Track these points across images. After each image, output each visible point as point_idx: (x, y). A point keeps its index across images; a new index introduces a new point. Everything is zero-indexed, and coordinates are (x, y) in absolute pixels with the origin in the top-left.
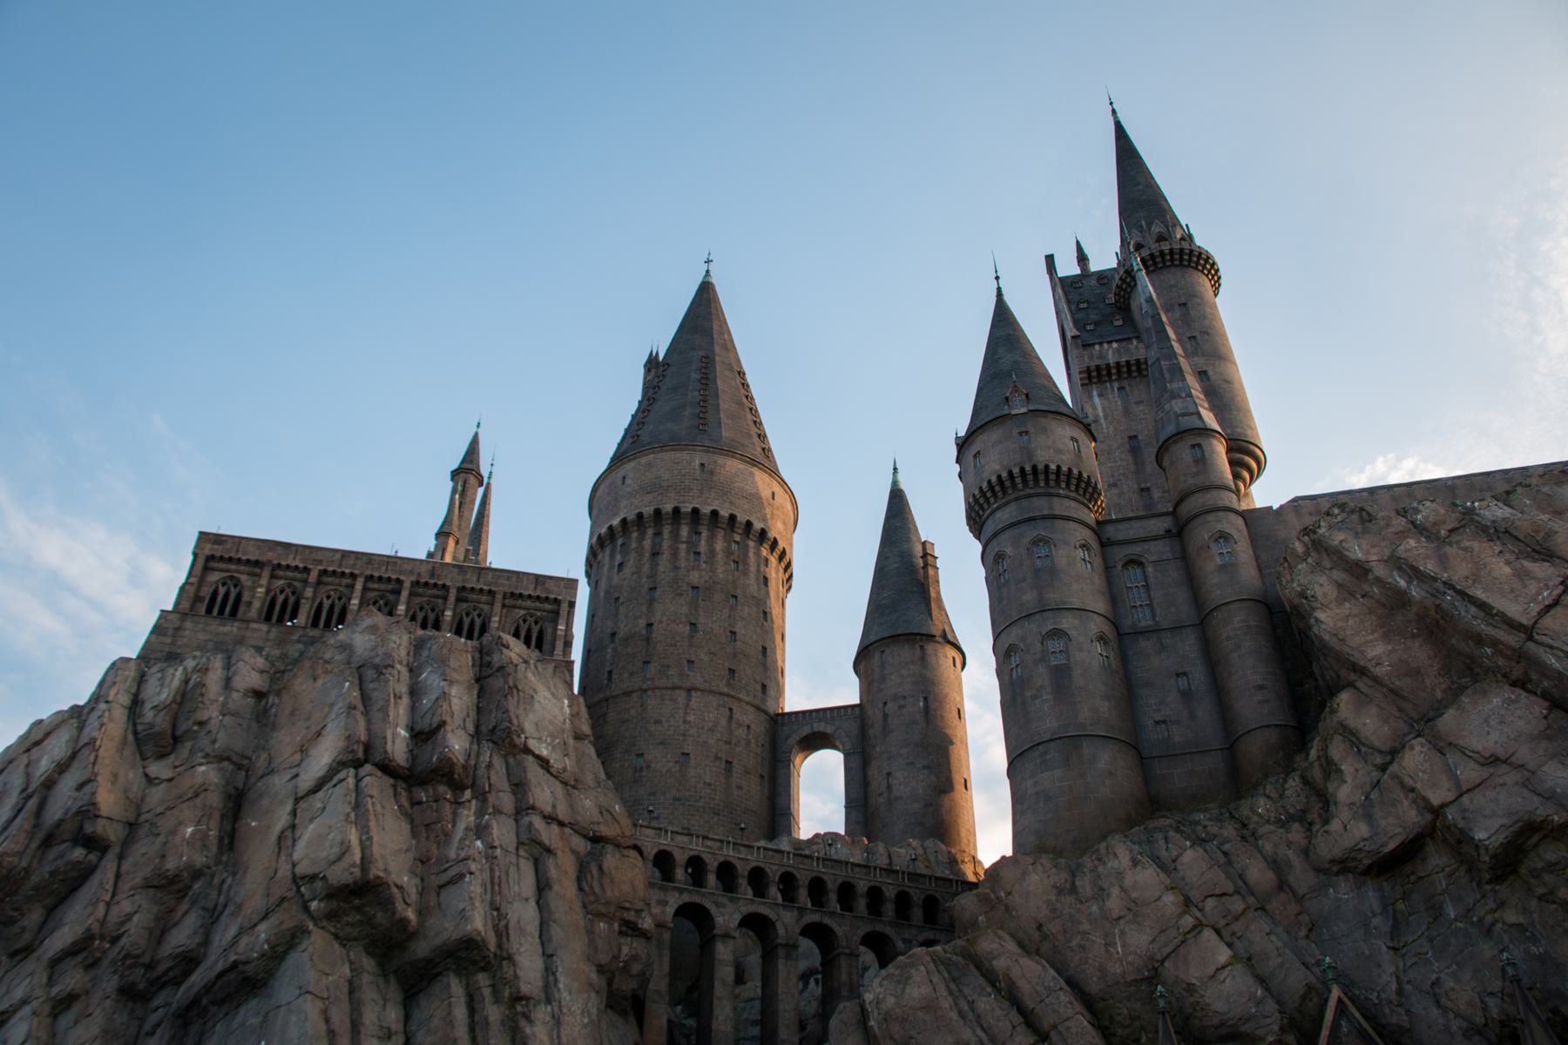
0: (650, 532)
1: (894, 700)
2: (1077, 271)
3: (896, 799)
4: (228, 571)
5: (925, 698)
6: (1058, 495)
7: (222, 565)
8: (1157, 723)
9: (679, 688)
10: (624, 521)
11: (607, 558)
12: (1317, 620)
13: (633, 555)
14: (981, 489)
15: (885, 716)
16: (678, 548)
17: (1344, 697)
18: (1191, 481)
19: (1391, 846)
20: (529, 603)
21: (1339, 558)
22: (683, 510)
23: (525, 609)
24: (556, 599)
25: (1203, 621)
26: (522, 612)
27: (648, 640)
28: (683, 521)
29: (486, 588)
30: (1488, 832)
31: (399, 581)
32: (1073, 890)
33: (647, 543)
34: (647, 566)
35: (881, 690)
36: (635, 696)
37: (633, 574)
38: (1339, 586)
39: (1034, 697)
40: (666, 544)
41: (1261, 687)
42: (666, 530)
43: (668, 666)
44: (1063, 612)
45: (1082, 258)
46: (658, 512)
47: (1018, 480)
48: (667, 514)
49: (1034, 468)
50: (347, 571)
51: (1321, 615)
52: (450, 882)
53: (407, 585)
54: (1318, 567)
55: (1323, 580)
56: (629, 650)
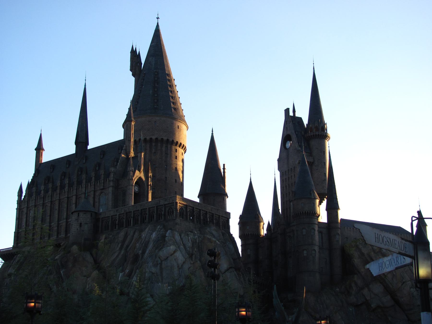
0: (164, 145)
10: (157, 139)
12: (354, 260)
14: (303, 212)
17: (356, 276)
19: (359, 304)
20: (223, 218)
23: (223, 219)
24: (228, 218)
26: (222, 220)
29: (219, 214)
30: (373, 306)
31: (207, 212)
33: (164, 149)
42: (169, 146)
46: (168, 140)
47: (311, 214)
50: (199, 208)
53: (208, 213)
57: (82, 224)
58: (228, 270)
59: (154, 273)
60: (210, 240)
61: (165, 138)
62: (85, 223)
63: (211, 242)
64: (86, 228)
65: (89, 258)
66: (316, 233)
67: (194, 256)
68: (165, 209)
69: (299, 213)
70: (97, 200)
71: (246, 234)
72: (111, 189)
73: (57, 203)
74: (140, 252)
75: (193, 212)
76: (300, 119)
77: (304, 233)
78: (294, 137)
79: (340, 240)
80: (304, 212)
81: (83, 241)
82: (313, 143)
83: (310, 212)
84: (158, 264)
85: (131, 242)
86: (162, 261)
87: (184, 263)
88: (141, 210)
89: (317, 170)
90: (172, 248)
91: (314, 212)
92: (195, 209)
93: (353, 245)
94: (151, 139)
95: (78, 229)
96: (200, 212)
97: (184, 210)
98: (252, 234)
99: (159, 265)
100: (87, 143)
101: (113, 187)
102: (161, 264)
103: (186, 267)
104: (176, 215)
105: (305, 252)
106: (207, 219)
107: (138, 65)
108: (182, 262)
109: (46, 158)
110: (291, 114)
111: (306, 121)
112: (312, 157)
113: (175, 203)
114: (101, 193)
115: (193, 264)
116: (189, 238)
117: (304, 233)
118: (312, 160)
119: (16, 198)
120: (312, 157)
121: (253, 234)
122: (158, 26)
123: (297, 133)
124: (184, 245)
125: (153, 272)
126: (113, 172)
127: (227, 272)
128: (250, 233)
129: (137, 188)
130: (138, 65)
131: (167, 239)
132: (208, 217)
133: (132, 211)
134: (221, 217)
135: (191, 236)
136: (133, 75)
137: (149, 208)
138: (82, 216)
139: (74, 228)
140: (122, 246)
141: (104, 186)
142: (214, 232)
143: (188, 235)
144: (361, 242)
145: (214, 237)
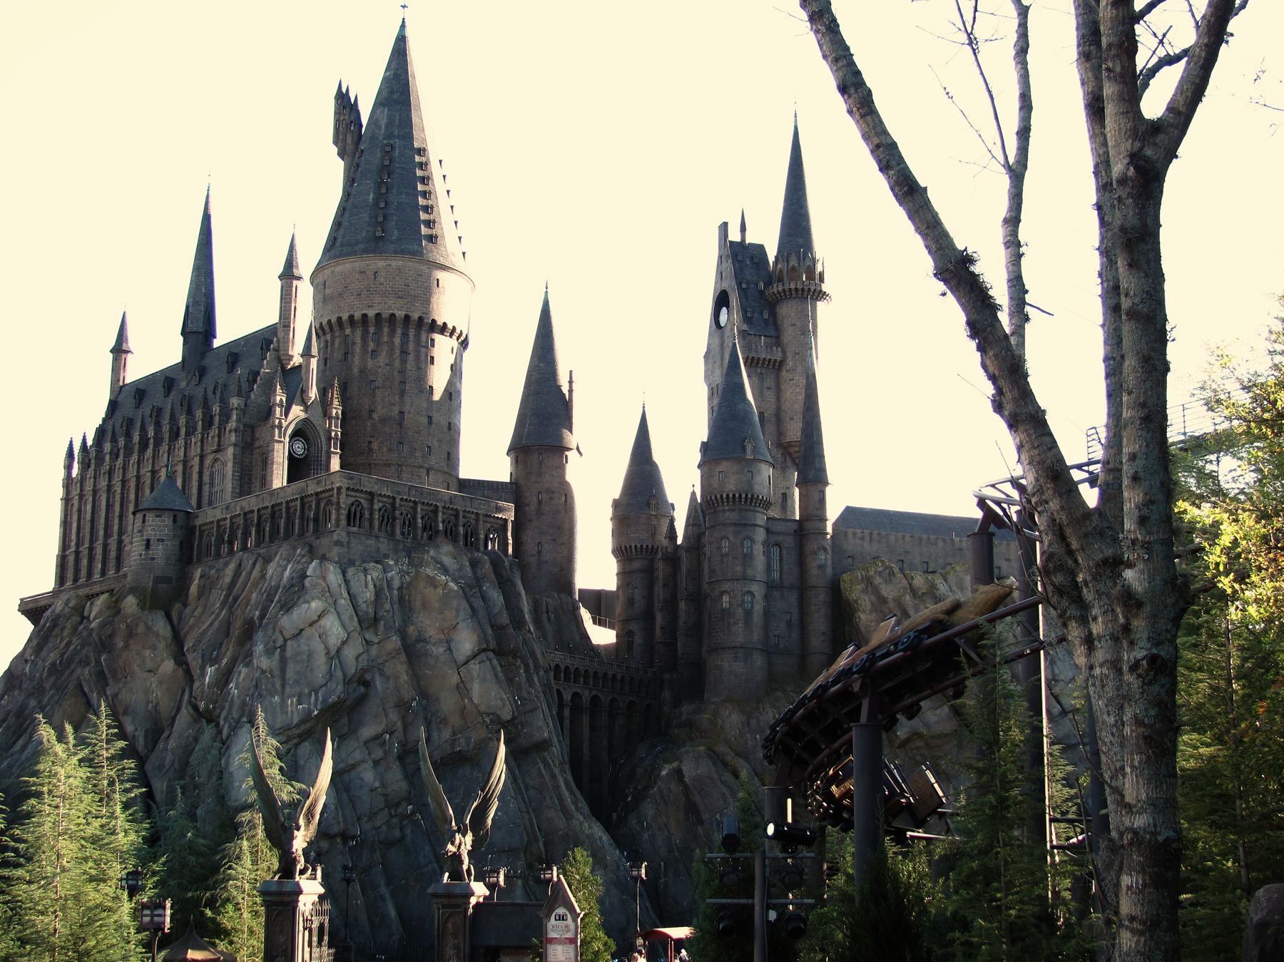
0: (399, 331)
1: (547, 492)
2: (739, 240)
3: (544, 562)
4: (356, 497)
5: (566, 495)
6: (759, 512)
7: (353, 494)
8: (775, 636)
9: (423, 467)
10: (378, 315)
11: (358, 340)
13: (385, 348)
15: (540, 502)
16: (419, 351)
18: (815, 512)
21: (876, 591)
22: (426, 321)
25: (803, 587)
26: (489, 525)
27: (401, 424)
28: (424, 329)
31: (436, 507)
32: (749, 724)
33: (397, 341)
34: (398, 361)
35: (538, 482)
36: (393, 467)
37: (387, 365)
38: (872, 604)
39: (735, 624)
40: (411, 346)
41: (824, 633)
42: (412, 332)
43: (415, 449)
44: (754, 582)
45: (743, 228)
46: (407, 317)
48: (414, 320)
49: (752, 496)
51: (863, 616)
52: (531, 711)
53: (440, 509)
54: (865, 591)
55: (866, 598)
56: (387, 429)
57: (151, 543)
58: (474, 656)
59: (266, 672)
60: (432, 582)
61: (400, 314)
62: (159, 540)
63: (435, 587)
64: (159, 551)
65: (161, 625)
66: (759, 550)
67: (382, 623)
68: (318, 504)
69: (713, 498)
70: (206, 478)
71: (623, 548)
72: (230, 451)
73: (132, 484)
74: (257, 613)
75: (394, 509)
76: (761, 249)
77: (725, 550)
78: (734, 300)
79: (829, 563)
80: (724, 496)
81: (151, 584)
82: (787, 311)
83: (740, 495)
84: (276, 649)
85: (243, 591)
86: (285, 640)
87: (344, 643)
88: (273, 506)
89: (791, 380)
90: (316, 605)
91: (749, 496)
92: (398, 501)
93: (860, 578)
94: (365, 316)
95: (141, 555)
96: (415, 509)
97: (365, 505)
98: (639, 546)
99: (279, 650)
100: (210, 332)
101: (235, 445)
102: (283, 648)
103: (350, 653)
104: (338, 521)
105: (726, 598)
106: (438, 525)
107: (352, 128)
108: (339, 641)
109: (135, 371)
110: (734, 236)
111: (772, 253)
112: (779, 349)
113: (335, 491)
114: (216, 460)
115: (378, 643)
116: (369, 577)
117: (725, 550)
118: (778, 356)
119: (61, 474)
120: (779, 349)
121: (642, 546)
122: (403, 26)
123: (744, 286)
124: (352, 597)
125: (264, 668)
126: (237, 409)
127: (473, 662)
128: (633, 545)
129: (301, 445)
130: (352, 128)
131: (307, 582)
132: (440, 519)
133: (256, 509)
134: (481, 517)
135: (375, 572)
136: (342, 154)
137: (287, 502)
138: (153, 521)
139: (134, 550)
140: (227, 596)
141: (219, 445)
142: (447, 561)
143: (365, 571)
144: (880, 569)
145: (445, 570)
